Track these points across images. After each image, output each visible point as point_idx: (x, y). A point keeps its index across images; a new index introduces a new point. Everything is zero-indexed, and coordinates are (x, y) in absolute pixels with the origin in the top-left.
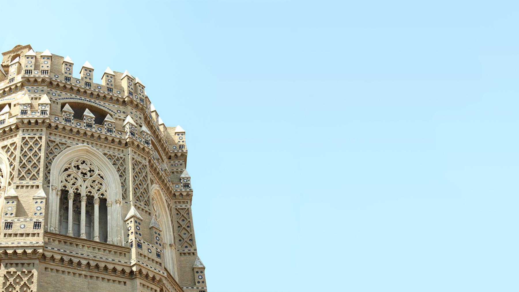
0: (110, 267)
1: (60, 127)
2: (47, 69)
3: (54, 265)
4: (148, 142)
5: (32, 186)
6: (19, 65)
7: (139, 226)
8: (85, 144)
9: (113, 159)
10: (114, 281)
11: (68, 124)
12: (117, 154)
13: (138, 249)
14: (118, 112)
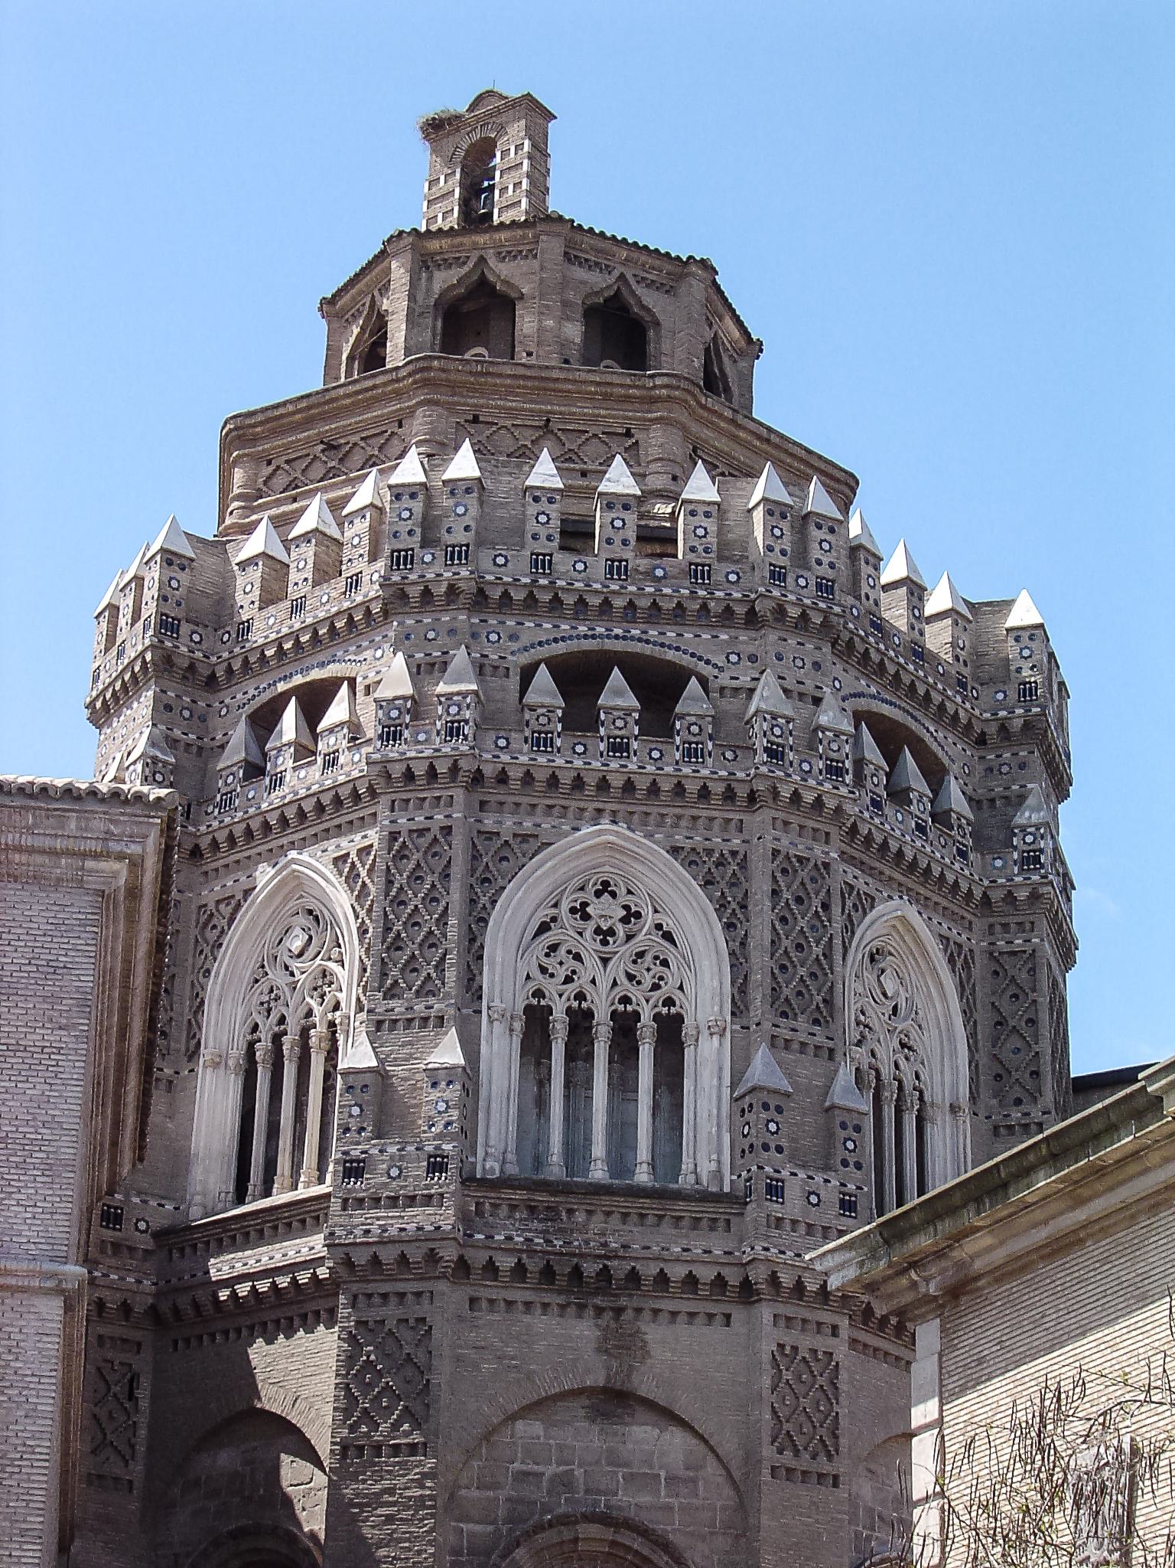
0: (678, 1272)
1: (515, 773)
2: (460, 537)
3: (496, 1287)
4: (840, 765)
5: (425, 1020)
6: (376, 514)
7: (778, 1118)
8: (605, 825)
9: (705, 862)
10: (692, 1315)
11: (542, 760)
12: (719, 840)
13: (768, 1203)
14: (729, 661)
